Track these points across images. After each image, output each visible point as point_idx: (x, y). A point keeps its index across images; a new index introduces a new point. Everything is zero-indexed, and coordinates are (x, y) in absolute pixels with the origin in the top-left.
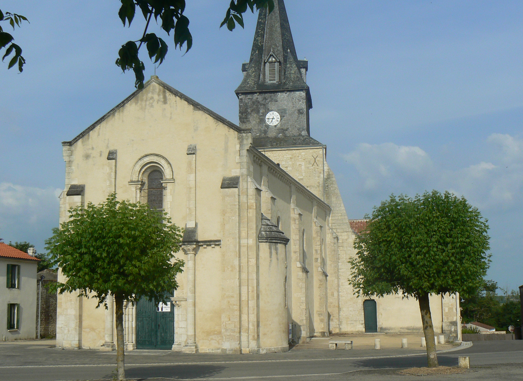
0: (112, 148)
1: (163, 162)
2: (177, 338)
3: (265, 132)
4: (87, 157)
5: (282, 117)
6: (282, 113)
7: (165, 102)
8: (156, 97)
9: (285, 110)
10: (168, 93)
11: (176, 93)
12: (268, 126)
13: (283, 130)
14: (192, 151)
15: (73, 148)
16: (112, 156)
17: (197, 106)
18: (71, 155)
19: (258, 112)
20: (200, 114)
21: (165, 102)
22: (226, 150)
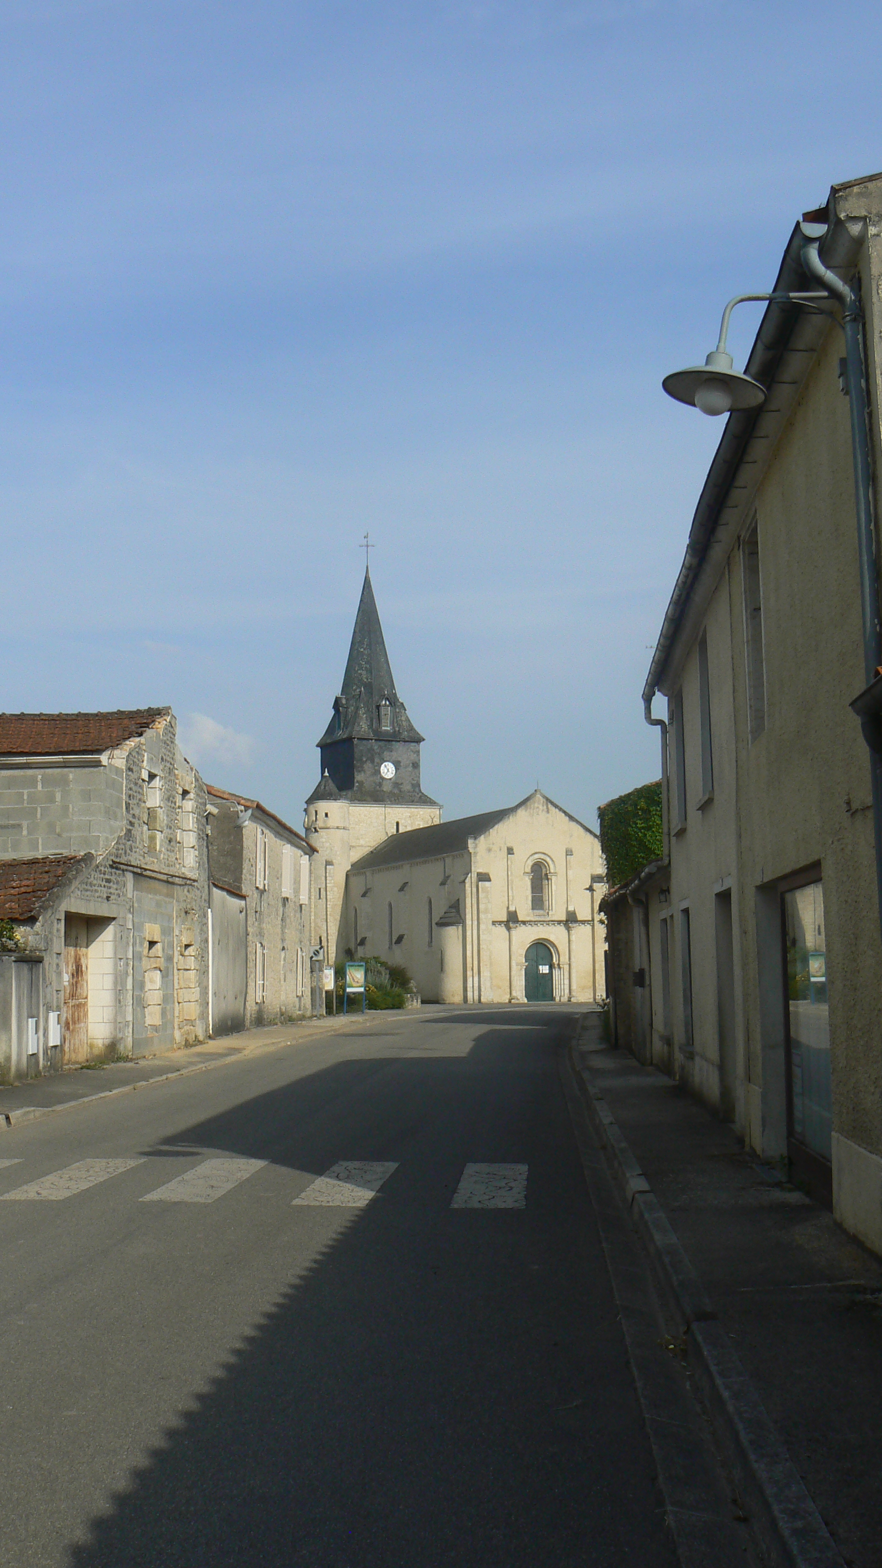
0: (509, 845)
1: (548, 859)
2: (557, 994)
3: (380, 785)
4: (489, 850)
5: (396, 769)
6: (397, 765)
7: (548, 812)
8: (541, 807)
9: (399, 762)
10: (550, 805)
11: (556, 806)
12: (383, 778)
13: (396, 783)
14: (569, 853)
15: (477, 841)
16: (510, 851)
17: (571, 818)
18: (476, 847)
19: (373, 762)
20: (573, 824)
21: (548, 812)
22: (592, 853)
